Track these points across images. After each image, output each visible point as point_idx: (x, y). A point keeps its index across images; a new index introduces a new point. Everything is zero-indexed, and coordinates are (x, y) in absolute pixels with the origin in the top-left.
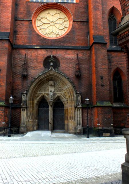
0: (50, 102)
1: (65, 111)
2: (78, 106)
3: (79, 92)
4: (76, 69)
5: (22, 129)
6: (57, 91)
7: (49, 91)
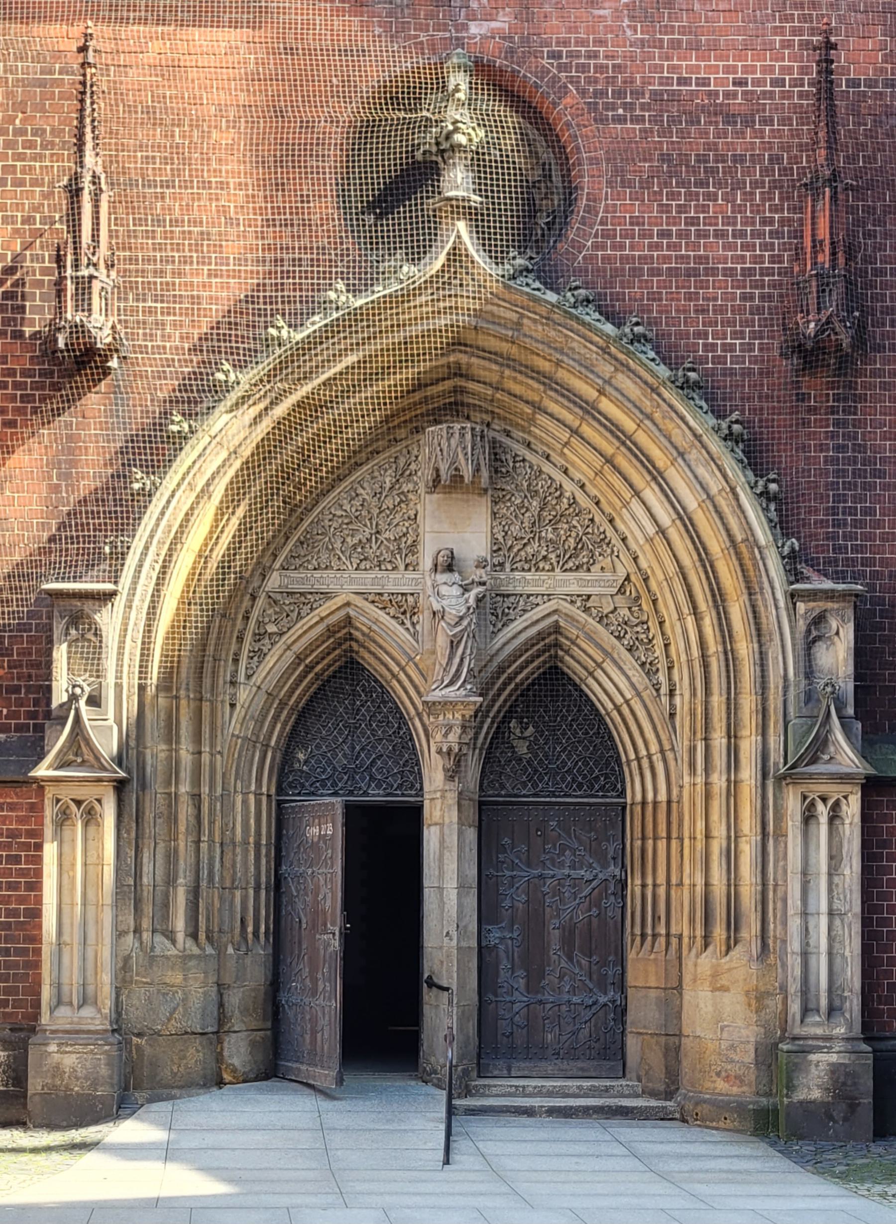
0: (431, 707)
1: (633, 826)
2: (814, 760)
3: (839, 577)
4: (798, 255)
5: (57, 1070)
6: (533, 564)
7: (427, 563)
